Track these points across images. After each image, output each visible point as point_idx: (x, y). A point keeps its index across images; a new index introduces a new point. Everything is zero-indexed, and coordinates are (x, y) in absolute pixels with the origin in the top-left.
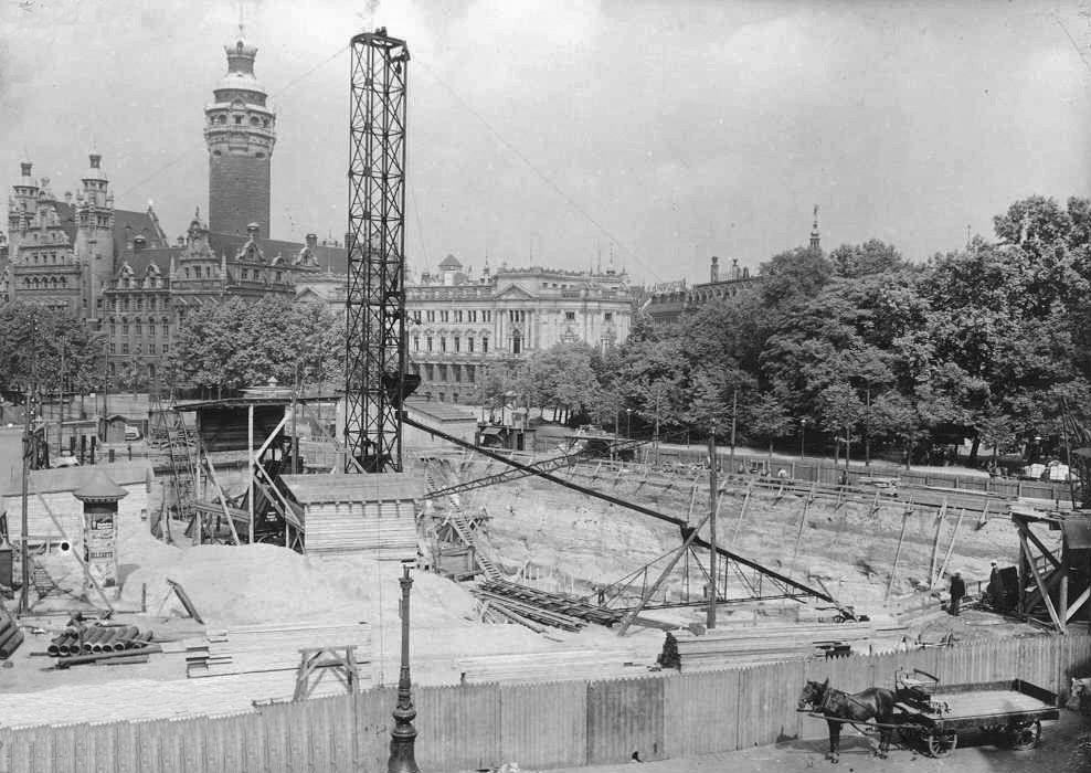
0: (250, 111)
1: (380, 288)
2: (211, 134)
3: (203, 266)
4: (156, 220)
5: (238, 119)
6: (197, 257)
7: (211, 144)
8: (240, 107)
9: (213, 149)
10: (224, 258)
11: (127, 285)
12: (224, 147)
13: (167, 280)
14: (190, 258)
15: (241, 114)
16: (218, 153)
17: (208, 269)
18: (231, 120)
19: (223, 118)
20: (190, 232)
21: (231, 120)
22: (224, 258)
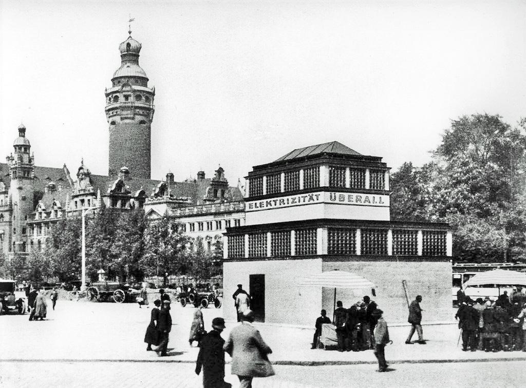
0: (134, 91)
1: (9, 205)
2: (109, 110)
3: (86, 199)
4: (69, 173)
5: (127, 97)
6: (82, 193)
7: (109, 117)
8: (128, 88)
9: (111, 120)
10: (99, 191)
11: (56, 215)
12: (117, 119)
13: (64, 211)
14: (78, 194)
15: (129, 93)
16: (113, 123)
17: (89, 200)
18: (122, 99)
19: (116, 99)
20: (78, 175)
21: (122, 99)
22: (99, 191)
